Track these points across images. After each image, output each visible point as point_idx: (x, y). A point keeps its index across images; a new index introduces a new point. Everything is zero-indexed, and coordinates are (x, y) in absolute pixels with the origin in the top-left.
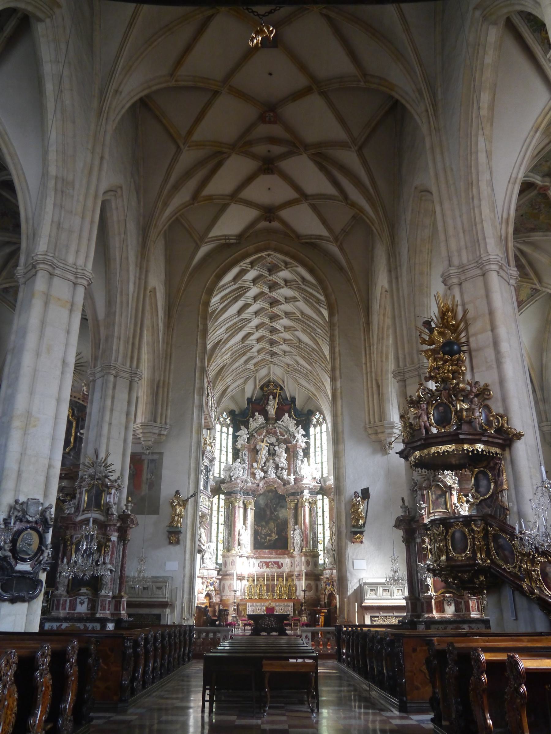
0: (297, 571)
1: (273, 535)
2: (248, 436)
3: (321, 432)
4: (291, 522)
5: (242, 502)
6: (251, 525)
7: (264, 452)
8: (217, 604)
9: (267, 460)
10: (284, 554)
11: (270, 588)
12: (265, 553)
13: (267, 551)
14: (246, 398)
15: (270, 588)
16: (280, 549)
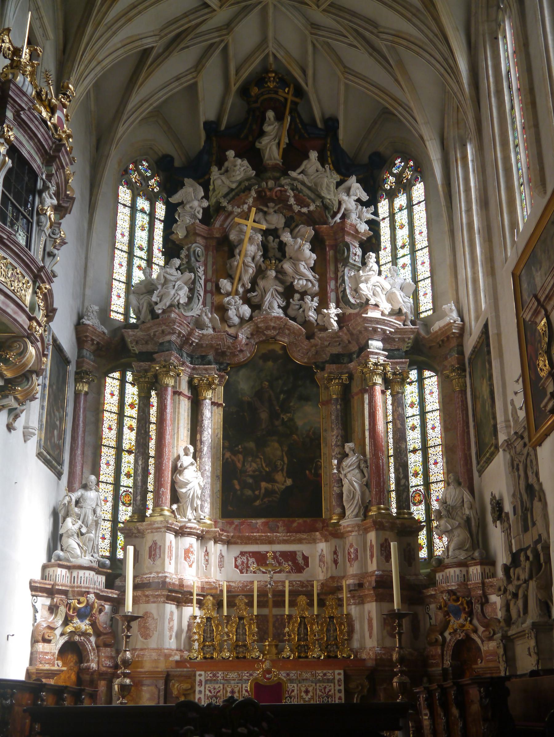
0: (354, 576)
1: (279, 477)
2: (205, 204)
3: (410, 206)
4: (332, 436)
5: (184, 380)
6: (213, 447)
7: (251, 249)
8: (101, 675)
9: (260, 273)
10: (312, 529)
11: (270, 629)
12: (254, 528)
13: (260, 522)
14: (202, 120)
15: (271, 629)
16: (299, 516)
